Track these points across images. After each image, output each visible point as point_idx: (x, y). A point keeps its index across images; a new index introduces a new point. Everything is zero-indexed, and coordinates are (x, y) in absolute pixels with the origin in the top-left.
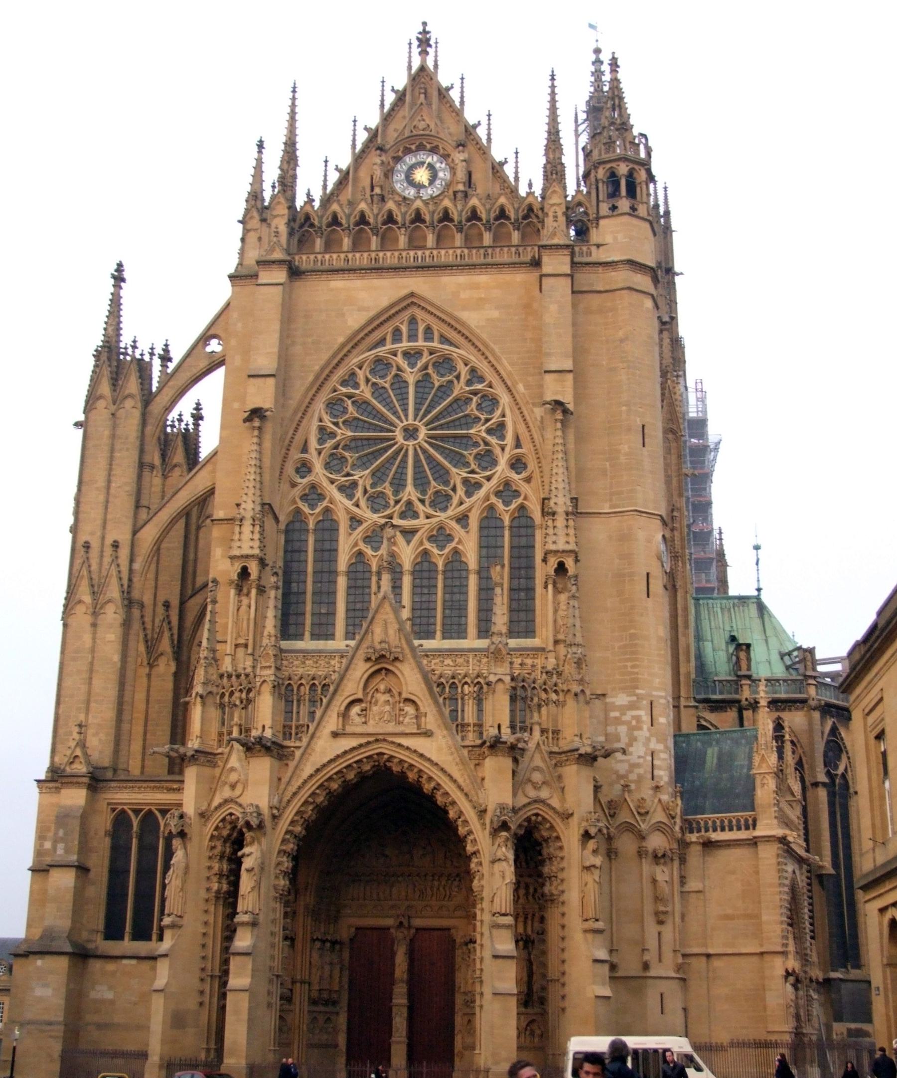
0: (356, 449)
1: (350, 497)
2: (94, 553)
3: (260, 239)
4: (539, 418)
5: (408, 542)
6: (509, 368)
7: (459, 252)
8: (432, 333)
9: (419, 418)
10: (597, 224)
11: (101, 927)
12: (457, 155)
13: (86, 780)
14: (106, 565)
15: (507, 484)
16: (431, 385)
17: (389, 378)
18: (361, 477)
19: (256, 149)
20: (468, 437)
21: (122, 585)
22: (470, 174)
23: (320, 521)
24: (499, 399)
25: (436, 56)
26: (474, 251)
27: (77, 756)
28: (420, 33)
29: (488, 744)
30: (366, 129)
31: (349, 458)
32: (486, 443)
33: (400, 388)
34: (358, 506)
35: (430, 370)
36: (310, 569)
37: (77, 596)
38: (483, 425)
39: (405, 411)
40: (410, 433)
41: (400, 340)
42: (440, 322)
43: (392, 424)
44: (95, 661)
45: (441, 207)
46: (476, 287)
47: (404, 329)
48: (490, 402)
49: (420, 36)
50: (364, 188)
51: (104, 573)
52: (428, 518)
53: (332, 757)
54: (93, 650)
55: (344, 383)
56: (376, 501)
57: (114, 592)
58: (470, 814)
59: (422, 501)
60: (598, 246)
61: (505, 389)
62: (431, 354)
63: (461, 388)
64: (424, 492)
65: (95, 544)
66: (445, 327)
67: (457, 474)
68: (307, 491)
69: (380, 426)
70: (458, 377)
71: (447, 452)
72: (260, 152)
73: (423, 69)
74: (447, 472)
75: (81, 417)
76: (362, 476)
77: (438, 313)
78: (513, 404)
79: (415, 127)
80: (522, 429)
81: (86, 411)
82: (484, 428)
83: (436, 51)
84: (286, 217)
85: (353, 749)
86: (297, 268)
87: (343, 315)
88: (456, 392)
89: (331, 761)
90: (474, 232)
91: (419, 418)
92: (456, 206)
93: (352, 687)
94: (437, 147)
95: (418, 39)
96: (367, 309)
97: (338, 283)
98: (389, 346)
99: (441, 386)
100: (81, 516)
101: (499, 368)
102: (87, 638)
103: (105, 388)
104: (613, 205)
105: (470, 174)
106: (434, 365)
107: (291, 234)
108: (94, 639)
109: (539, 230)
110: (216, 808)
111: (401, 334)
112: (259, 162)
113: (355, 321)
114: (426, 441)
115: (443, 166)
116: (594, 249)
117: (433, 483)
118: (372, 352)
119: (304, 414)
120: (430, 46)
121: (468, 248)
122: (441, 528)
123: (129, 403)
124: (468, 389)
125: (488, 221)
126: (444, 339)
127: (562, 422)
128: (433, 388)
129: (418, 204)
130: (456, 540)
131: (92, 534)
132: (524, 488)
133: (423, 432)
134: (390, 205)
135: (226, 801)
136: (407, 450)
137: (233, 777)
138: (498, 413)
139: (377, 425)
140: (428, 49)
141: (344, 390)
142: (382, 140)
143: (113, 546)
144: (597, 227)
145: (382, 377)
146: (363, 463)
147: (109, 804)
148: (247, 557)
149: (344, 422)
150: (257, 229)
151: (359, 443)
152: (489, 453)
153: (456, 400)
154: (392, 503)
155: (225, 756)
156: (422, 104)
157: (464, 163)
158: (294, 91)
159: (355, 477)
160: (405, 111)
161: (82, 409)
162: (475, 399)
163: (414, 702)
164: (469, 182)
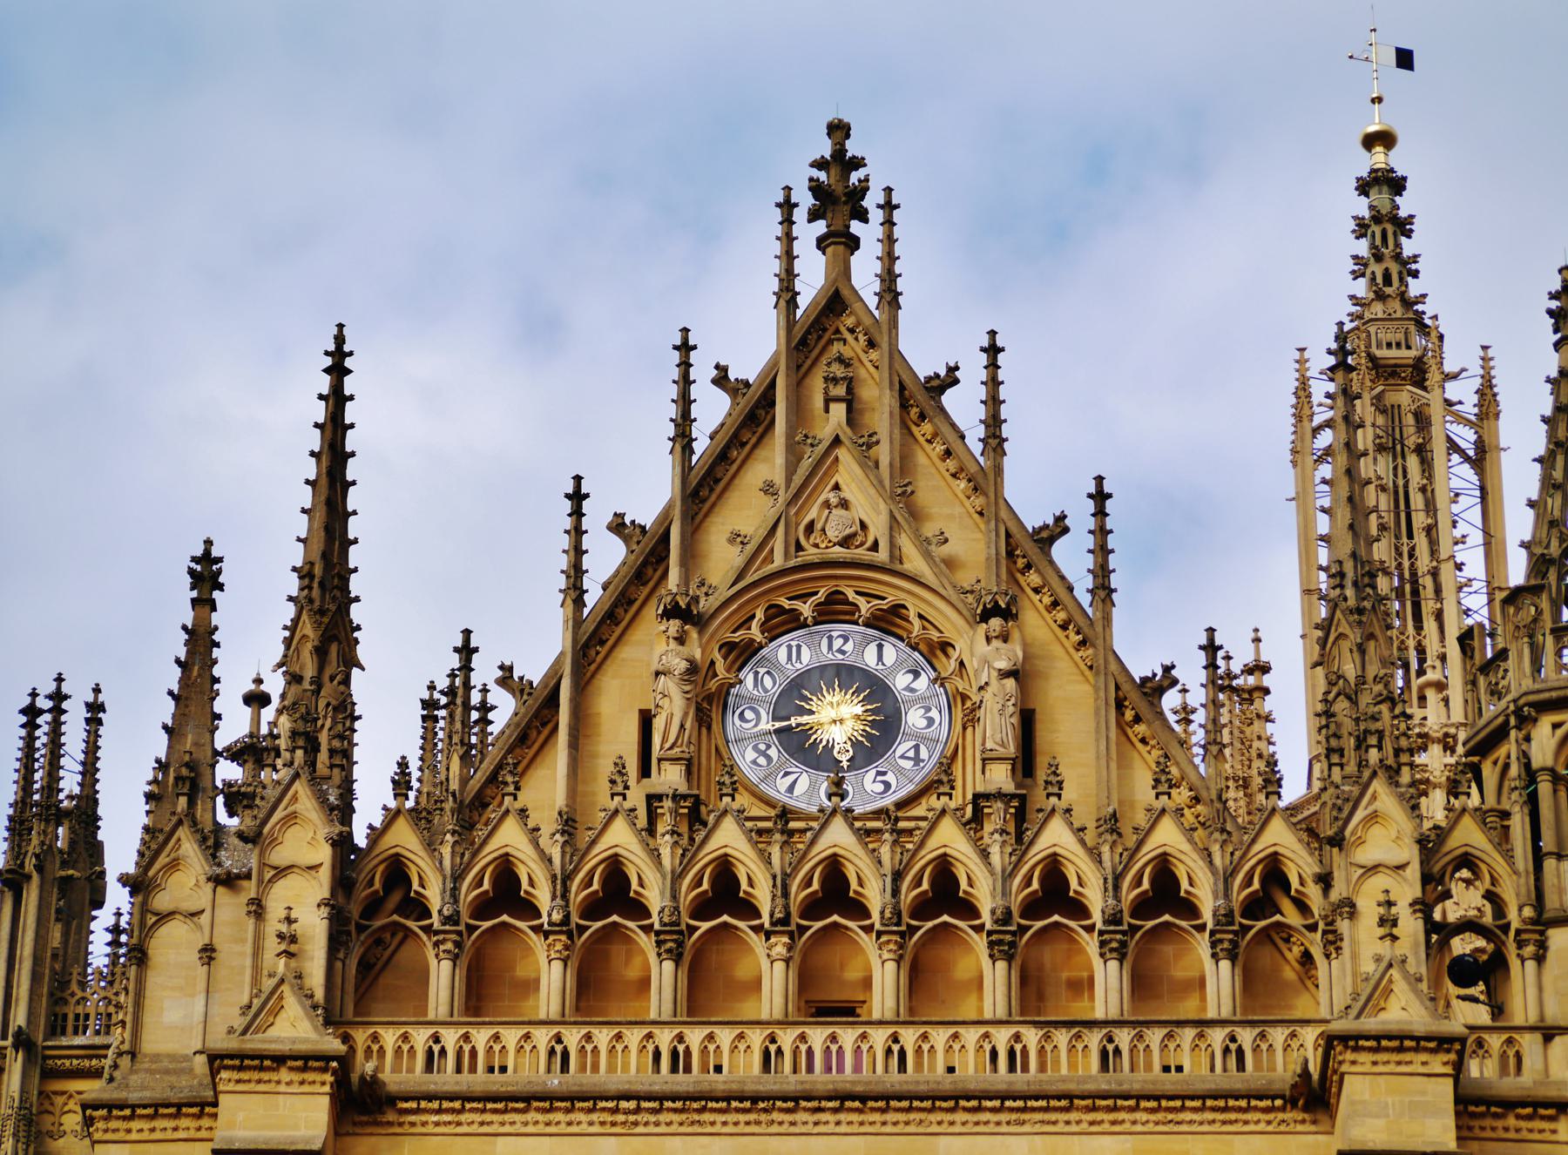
3: (208, 953)
7: (1002, 1037)
10: (1542, 945)
12: (981, 647)
19: (185, 593)
22: (1027, 722)
25: (890, 258)
26: (1062, 1037)
28: (820, 164)
30: (618, 526)
45: (928, 854)
49: (822, 176)
50: (621, 768)
60: (1549, 1034)
72: (205, 604)
73: (836, 301)
79: (810, 528)
83: (889, 240)
84: (325, 874)
86: (372, 1084)
90: (1050, 955)
92: (984, 854)
94: (897, 610)
95: (816, 188)
105: (1027, 722)
107: (336, 942)
109: (1307, 958)
112: (201, 641)
115: (922, 683)
116: (1529, 1043)
120: (863, 216)
121: (1036, 1024)
125: (1114, 919)
129: (838, 837)
134: (728, 838)
140: (856, 227)
142: (686, 579)
144: (1540, 959)
156: (837, 441)
157: (1010, 683)
158: (338, 370)
160: (769, 464)
164: (1025, 760)
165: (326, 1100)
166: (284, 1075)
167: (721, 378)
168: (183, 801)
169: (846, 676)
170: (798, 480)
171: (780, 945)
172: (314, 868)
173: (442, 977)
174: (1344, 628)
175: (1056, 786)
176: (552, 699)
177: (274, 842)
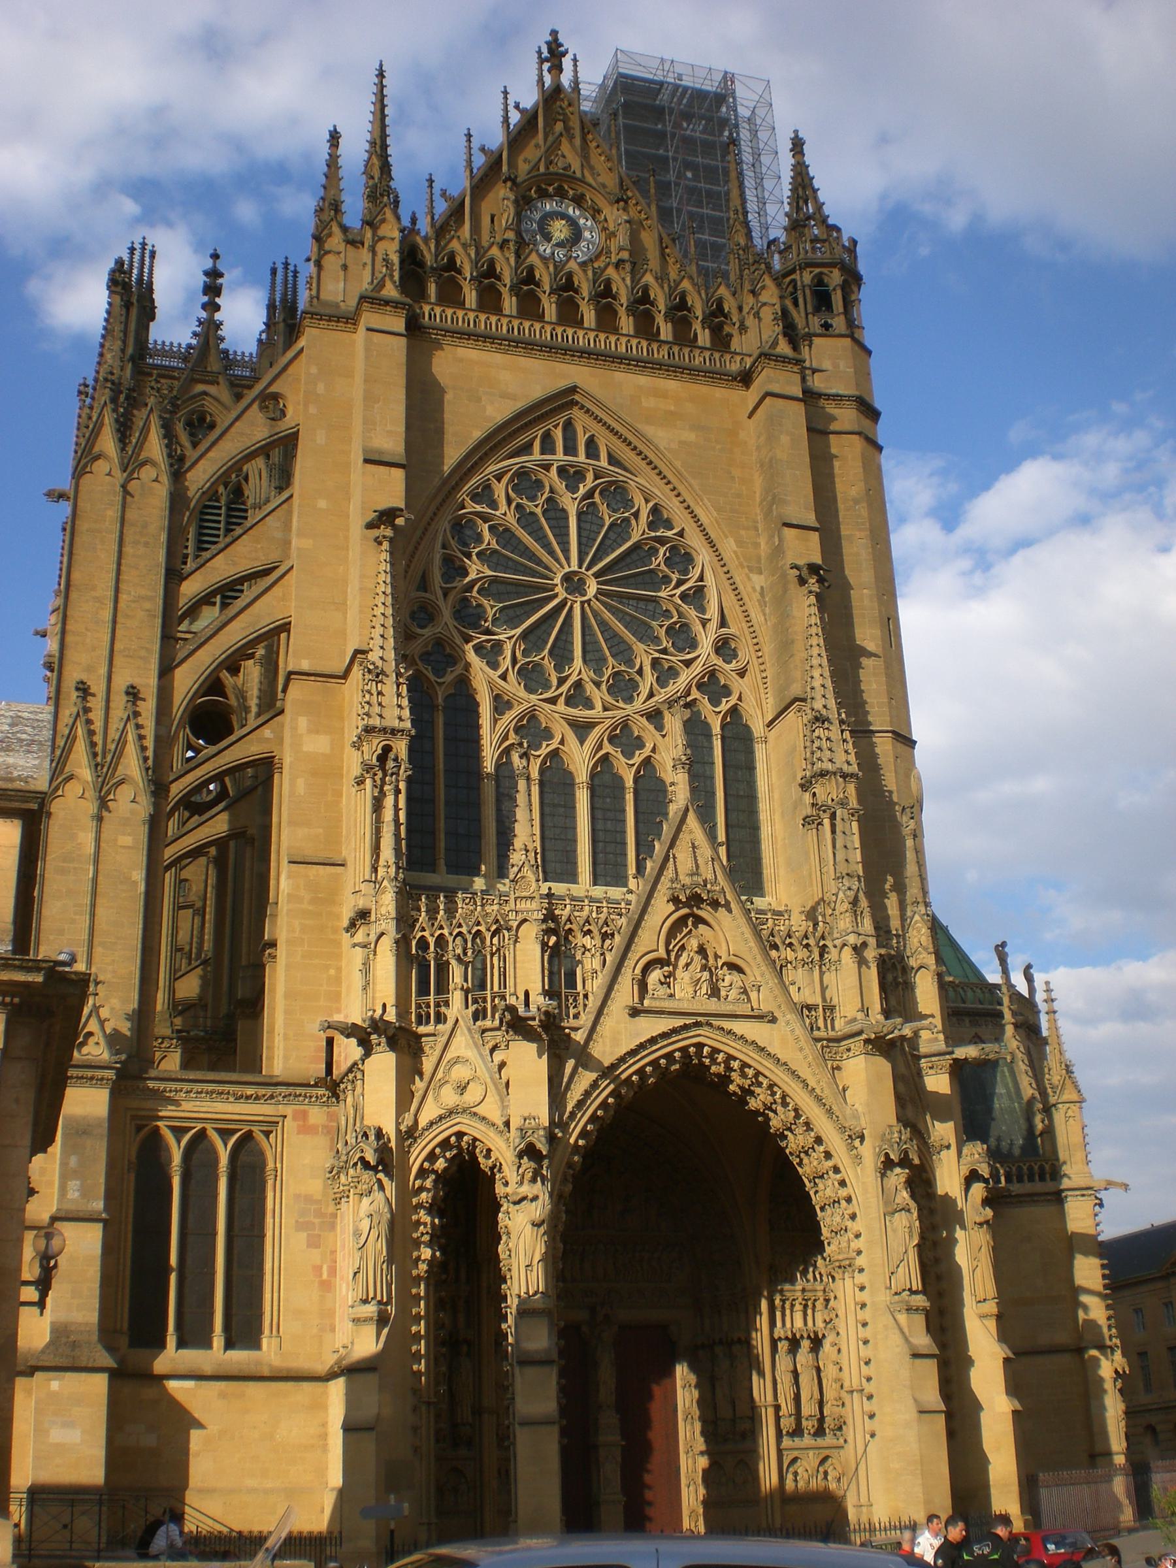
0: (498, 597)
1: (494, 665)
2: (96, 704)
4: (758, 588)
5: (582, 743)
6: (715, 514)
8: (597, 448)
9: (585, 565)
11: (126, 1325)
13: (110, 1074)
14: (115, 725)
15: (712, 674)
16: (599, 522)
17: (540, 501)
18: (510, 638)
20: (655, 600)
21: (146, 759)
23: (450, 695)
24: (694, 554)
27: (90, 1034)
29: (864, 1036)
30: (483, 149)
31: (489, 609)
32: (680, 615)
33: (556, 519)
34: (504, 677)
35: (597, 498)
36: (441, 766)
37: (67, 769)
38: (677, 586)
39: (566, 551)
40: (574, 583)
41: (553, 452)
42: (610, 435)
43: (547, 568)
44: (100, 878)
46: (664, 395)
47: (558, 435)
48: (681, 559)
51: (113, 734)
52: (605, 709)
53: (633, 1046)
54: (96, 862)
55: (475, 497)
56: (532, 677)
57: (132, 765)
58: (835, 1141)
59: (598, 685)
60: (814, 371)
61: (705, 543)
62: (596, 477)
63: (638, 531)
64: (599, 672)
65: (98, 687)
66: (619, 442)
67: (643, 655)
68: (429, 648)
69: (530, 568)
70: (636, 515)
71: (628, 618)
74: (630, 648)
75: (65, 483)
76: (508, 636)
77: (610, 421)
78: (718, 565)
80: (730, 601)
81: (79, 472)
82: (678, 592)
84: (397, 242)
85: (664, 1035)
87: (479, 400)
88: (635, 537)
89: (633, 1053)
91: (585, 565)
92: (624, 279)
93: (650, 940)
96: (514, 398)
97: (469, 354)
98: (536, 455)
99: (612, 525)
100: (69, 639)
101: (699, 511)
102: (87, 839)
103: (108, 443)
104: (826, 322)
106: (601, 493)
108: (98, 840)
110: (432, 1124)
111: (553, 443)
113: (498, 412)
114: (597, 599)
117: (610, 659)
118: (517, 460)
119: (424, 533)
122: (625, 725)
123: (148, 473)
124: (653, 534)
126: (612, 460)
127: (818, 596)
128: (603, 526)
130: (649, 746)
131: (90, 669)
132: (738, 685)
133: (592, 587)
135: (451, 1113)
136: (571, 607)
137: (460, 1073)
138: (696, 573)
139: (526, 566)
141: (478, 508)
143: (128, 693)
144: (810, 346)
145: (532, 498)
146: (511, 617)
147: (133, 1118)
148: (394, 732)
149: (478, 555)
150: (339, 253)
151: (502, 588)
152: (685, 627)
153: (637, 547)
154: (555, 682)
155: (444, 1039)
156: (561, 135)
159: (501, 637)
161: (70, 470)
162: (662, 551)
163: (740, 970)
165: (403, 320)
166: (388, 308)
167: (517, 106)
168: (332, 213)
169: (564, 216)
170: (549, 143)
171: (554, 298)
172: (393, 239)
173: (432, 289)
174: (739, 227)
175: (646, 261)
176: (462, 203)
177: (378, 228)
